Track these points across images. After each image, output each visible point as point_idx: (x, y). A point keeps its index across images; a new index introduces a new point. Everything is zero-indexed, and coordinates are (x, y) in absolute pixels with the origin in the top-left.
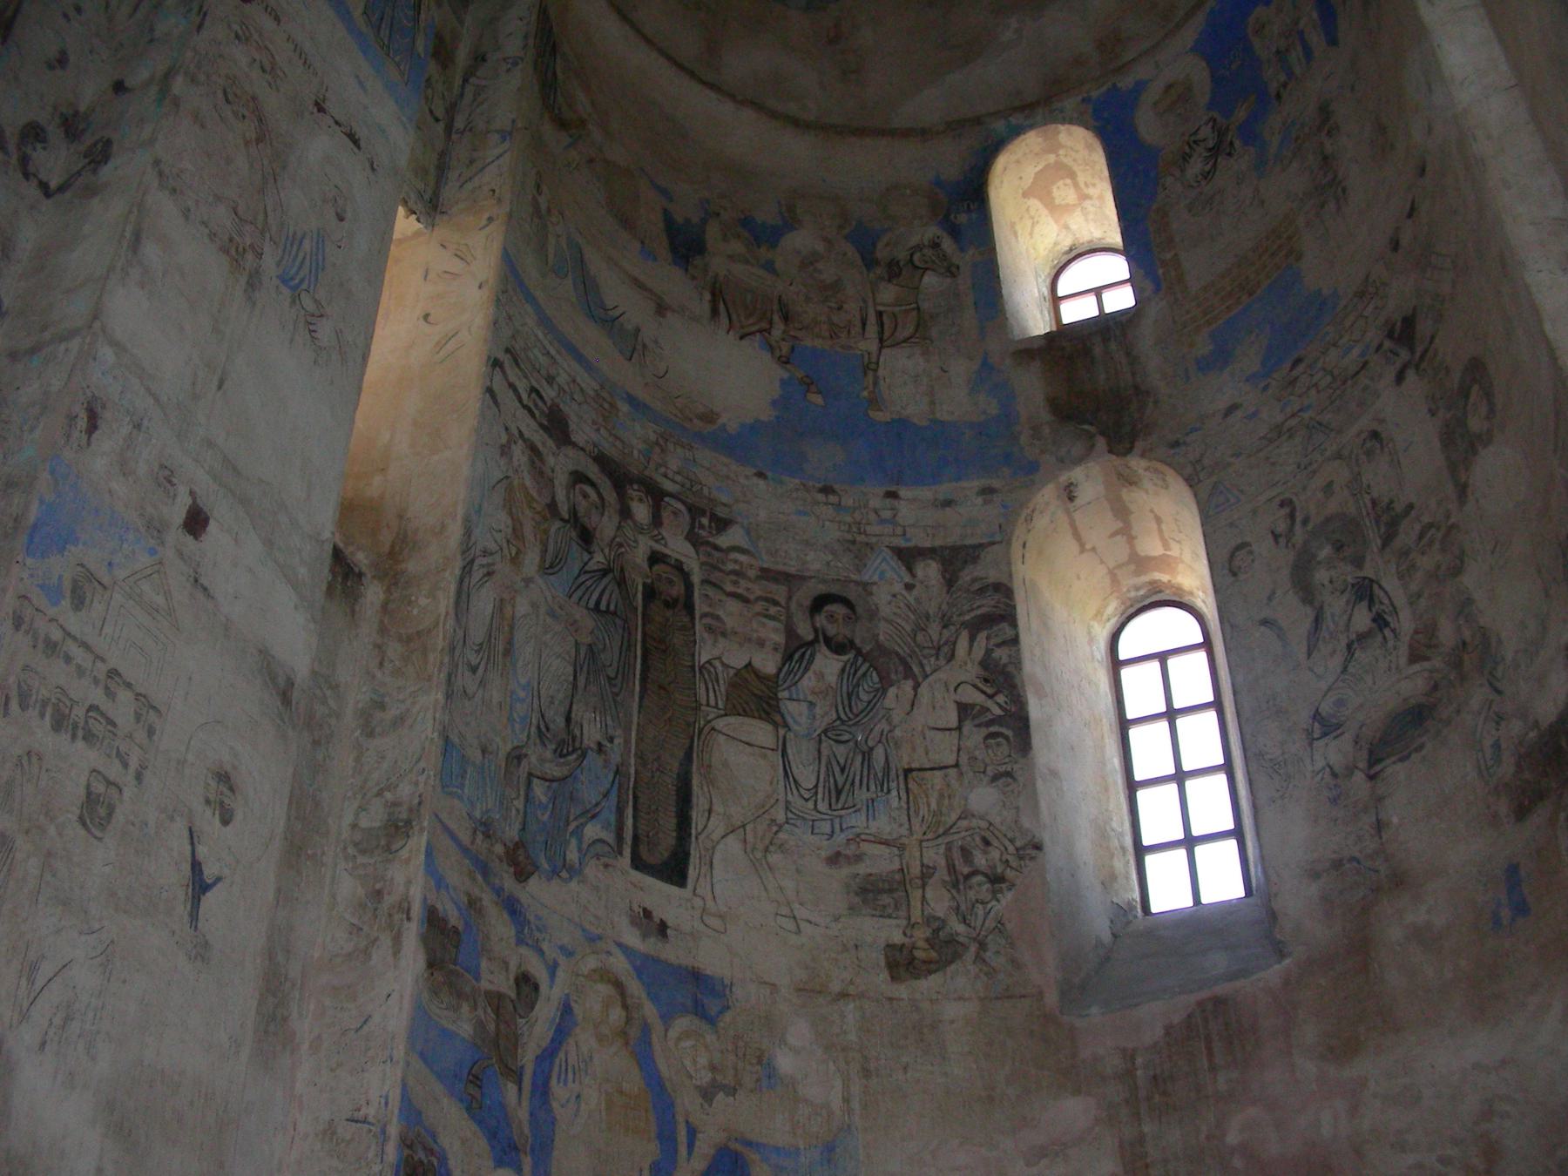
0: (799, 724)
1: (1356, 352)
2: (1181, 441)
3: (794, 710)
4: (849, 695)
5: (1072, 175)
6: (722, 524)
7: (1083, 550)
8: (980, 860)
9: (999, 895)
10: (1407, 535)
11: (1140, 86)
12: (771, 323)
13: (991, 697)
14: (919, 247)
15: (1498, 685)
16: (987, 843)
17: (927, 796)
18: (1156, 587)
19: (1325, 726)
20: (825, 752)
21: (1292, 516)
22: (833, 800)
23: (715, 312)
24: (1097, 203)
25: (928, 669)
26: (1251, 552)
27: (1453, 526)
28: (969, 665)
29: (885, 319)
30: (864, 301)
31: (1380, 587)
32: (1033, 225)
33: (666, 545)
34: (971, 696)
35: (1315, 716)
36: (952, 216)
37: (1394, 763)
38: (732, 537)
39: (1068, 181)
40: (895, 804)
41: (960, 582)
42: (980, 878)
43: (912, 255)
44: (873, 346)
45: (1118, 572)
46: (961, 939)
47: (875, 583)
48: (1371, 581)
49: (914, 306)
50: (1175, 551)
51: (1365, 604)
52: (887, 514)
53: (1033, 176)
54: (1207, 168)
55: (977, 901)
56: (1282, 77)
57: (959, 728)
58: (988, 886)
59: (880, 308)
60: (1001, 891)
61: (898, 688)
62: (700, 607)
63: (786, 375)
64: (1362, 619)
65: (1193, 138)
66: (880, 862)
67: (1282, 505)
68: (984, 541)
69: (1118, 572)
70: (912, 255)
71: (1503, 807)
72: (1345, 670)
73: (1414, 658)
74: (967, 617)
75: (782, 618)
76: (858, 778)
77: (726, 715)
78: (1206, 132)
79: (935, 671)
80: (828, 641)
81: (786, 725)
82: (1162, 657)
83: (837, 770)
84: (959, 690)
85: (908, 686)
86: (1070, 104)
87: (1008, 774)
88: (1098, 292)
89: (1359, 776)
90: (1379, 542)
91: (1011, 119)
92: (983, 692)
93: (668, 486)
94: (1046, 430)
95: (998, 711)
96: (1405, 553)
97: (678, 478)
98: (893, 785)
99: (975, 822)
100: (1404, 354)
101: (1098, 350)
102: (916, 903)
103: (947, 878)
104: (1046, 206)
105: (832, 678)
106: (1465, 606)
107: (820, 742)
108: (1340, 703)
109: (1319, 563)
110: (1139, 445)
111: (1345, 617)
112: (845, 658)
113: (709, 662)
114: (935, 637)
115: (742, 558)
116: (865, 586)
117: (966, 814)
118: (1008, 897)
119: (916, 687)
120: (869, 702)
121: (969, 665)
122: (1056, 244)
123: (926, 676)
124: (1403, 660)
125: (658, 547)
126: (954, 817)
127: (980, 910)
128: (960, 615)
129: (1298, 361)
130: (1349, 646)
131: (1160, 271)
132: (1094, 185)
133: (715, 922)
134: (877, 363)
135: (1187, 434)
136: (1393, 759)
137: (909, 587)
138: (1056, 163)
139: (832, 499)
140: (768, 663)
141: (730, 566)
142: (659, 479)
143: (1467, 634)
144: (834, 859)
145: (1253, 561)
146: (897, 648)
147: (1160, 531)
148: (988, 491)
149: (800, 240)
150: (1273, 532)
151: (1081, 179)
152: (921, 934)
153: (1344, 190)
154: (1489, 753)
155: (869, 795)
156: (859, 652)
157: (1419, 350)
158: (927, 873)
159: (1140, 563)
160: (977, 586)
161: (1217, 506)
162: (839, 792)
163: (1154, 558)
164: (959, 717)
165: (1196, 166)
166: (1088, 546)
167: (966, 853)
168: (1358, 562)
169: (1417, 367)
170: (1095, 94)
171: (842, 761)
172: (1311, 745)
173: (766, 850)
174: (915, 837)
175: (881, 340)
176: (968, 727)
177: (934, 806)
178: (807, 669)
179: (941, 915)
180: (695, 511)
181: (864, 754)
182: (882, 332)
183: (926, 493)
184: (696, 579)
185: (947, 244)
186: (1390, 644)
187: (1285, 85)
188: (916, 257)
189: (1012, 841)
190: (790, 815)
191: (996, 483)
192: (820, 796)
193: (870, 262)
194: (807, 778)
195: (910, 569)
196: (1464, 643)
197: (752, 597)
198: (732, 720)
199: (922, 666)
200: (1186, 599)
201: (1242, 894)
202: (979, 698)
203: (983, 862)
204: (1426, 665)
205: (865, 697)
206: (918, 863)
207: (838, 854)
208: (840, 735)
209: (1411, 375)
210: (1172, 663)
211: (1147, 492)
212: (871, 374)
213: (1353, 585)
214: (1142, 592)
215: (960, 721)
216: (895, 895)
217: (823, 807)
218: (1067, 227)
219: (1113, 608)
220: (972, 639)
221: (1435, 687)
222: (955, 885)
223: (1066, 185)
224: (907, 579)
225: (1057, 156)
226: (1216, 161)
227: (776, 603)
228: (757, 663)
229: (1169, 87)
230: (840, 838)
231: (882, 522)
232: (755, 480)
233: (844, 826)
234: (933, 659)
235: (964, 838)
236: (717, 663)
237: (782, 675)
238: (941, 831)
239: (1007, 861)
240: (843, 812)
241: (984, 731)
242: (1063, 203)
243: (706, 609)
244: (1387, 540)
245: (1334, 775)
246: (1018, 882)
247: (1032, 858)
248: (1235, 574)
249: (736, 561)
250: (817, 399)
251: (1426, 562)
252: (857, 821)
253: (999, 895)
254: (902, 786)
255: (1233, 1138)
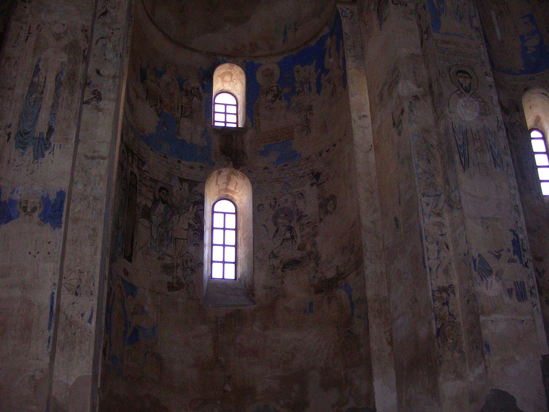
0: (154, 221)
1: (302, 172)
2: (252, 171)
3: (154, 218)
4: (165, 216)
5: (232, 75)
6: (144, 163)
7: (216, 185)
8: (189, 265)
9: (193, 274)
10: (304, 221)
11: (260, 65)
12: (157, 103)
13: (196, 223)
14: (193, 88)
15: (318, 264)
16: (191, 260)
17: (179, 246)
18: (227, 196)
19: (274, 256)
20: (159, 230)
21: (276, 202)
22: (160, 243)
23: (147, 97)
24: (234, 83)
25: (183, 213)
26: (263, 207)
27: (315, 226)
28: (192, 214)
29: (183, 108)
30: (179, 101)
31: (294, 229)
32: (217, 83)
33: (133, 169)
34: (192, 222)
35: (272, 252)
36: (203, 81)
37: (289, 270)
38: (145, 168)
39: (230, 76)
40: (173, 247)
41: (192, 191)
42: (189, 269)
43: (192, 90)
44: (179, 115)
45: (221, 191)
46: (184, 283)
47: (173, 186)
48: (292, 227)
49: (190, 106)
50: (237, 191)
51: (289, 232)
52: (178, 167)
53: (222, 72)
54: (273, 99)
55: (188, 274)
56: (301, 89)
57: (188, 230)
58: (190, 271)
59: (183, 105)
60: (193, 273)
61: (176, 216)
62: (138, 188)
63: (159, 120)
64: (288, 235)
65: (271, 88)
66: (168, 261)
67: (274, 199)
68: (199, 181)
69: (221, 191)
70: (192, 90)
71: (312, 290)
72: (281, 245)
73: (299, 249)
74: (193, 201)
75: (153, 192)
76: (165, 238)
77: (141, 218)
78: (275, 88)
79: (184, 213)
80: (162, 200)
81: (152, 222)
82: (225, 213)
83: (161, 235)
84: (189, 220)
85: (178, 216)
86: (240, 60)
87: (198, 244)
88: (226, 105)
89: (280, 270)
90: (297, 220)
91: (224, 57)
92: (195, 222)
93: (135, 152)
94: (218, 155)
95: (197, 227)
96: (303, 225)
97: (137, 149)
98: (173, 241)
99: (189, 255)
100: (315, 181)
101: (234, 137)
102: (175, 273)
103: (182, 268)
104: (221, 79)
105: (162, 211)
106: (314, 244)
107: (158, 227)
108: (279, 252)
109: (280, 217)
110: (241, 168)
111: (284, 233)
112: (165, 205)
113: (139, 203)
114: (185, 204)
115: (146, 174)
116: (171, 186)
117: (187, 252)
118: (195, 275)
119: (180, 217)
120: (169, 218)
121: (192, 214)
122: (219, 88)
123: (182, 214)
124: (296, 249)
125: (132, 170)
126: (185, 253)
127: (188, 277)
128: (192, 200)
129: (286, 165)
130: (284, 240)
131: (254, 122)
132: (236, 80)
133: (135, 272)
134: (180, 121)
135: (254, 170)
136: (289, 269)
137: (181, 189)
138: (230, 72)
139: (166, 160)
140: (149, 204)
141: (144, 176)
142: (134, 150)
143: (313, 251)
144: (159, 258)
145: (264, 209)
146: (177, 206)
147: (236, 186)
148: (201, 167)
149: (166, 77)
150: (270, 205)
151: (233, 77)
152: (175, 280)
153: (310, 131)
154: (312, 277)
155: (167, 243)
156: (168, 205)
157: (319, 183)
158: (178, 266)
159: (227, 190)
160: (196, 193)
161: (257, 192)
162: (161, 241)
163: (231, 190)
164: (188, 227)
165: (270, 97)
166: (218, 184)
167: (186, 262)
168: (290, 222)
169: (317, 186)
170: (247, 61)
171: (162, 233)
172: (270, 258)
173: (146, 255)
174: (176, 256)
175: (181, 115)
176: (190, 230)
177: (181, 248)
178: (157, 208)
179: (180, 276)
180: (139, 159)
181: (167, 232)
182: (182, 112)
183: (187, 163)
184: (138, 179)
185: (201, 89)
186: (294, 243)
187: (301, 92)
188: (193, 91)
189: (197, 261)
190: (151, 246)
191: (203, 165)
192: (157, 241)
193: (181, 89)
194: (155, 237)
195: (181, 184)
196: (312, 252)
197: (148, 185)
198: (142, 219)
199: (181, 211)
200: (233, 200)
201: (234, 278)
202: (194, 223)
203: (190, 265)
204: (303, 252)
205: (169, 217)
206: (176, 263)
207: (160, 257)
208: (162, 226)
209: (315, 186)
210: (227, 215)
211: (238, 178)
212: (178, 124)
213: (288, 226)
214: (223, 196)
215: (189, 227)
216: (171, 270)
217: (157, 244)
218: (223, 85)
219: (216, 198)
220: (193, 207)
221: (302, 258)
222: (183, 270)
223: (229, 77)
224: (180, 186)
225: (231, 70)
226: (276, 99)
227: (152, 188)
228: (147, 204)
229: (268, 69)
230: (161, 253)
231: (176, 169)
232: (151, 151)
233: (162, 250)
234: (184, 210)
235: (186, 258)
236: (140, 203)
237: (152, 208)
238: (182, 255)
239: (195, 266)
240: (162, 247)
241: (194, 232)
242: (226, 80)
243: (139, 188)
244: (299, 220)
245: (274, 267)
246: (197, 272)
247: (201, 267)
248: (259, 211)
249: (145, 175)
250: (165, 129)
251: (307, 230)
252: (164, 249)
253: (193, 274)
254: (174, 242)
255: (237, 341)
